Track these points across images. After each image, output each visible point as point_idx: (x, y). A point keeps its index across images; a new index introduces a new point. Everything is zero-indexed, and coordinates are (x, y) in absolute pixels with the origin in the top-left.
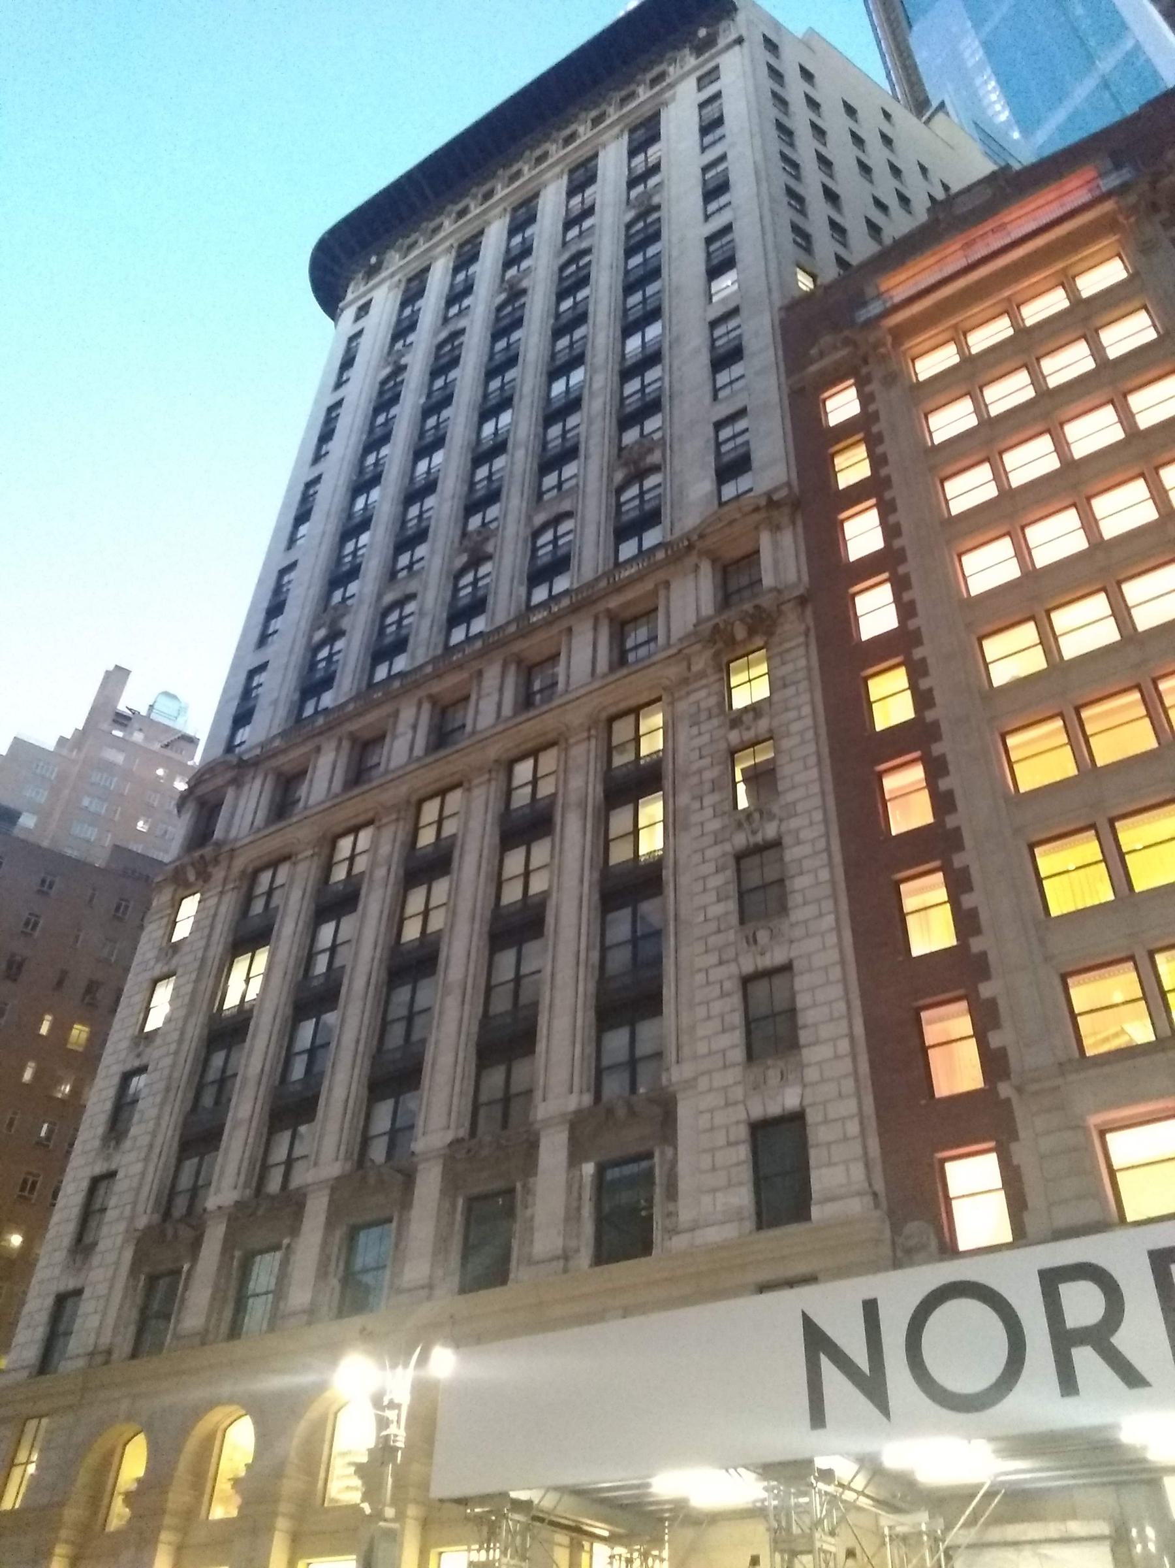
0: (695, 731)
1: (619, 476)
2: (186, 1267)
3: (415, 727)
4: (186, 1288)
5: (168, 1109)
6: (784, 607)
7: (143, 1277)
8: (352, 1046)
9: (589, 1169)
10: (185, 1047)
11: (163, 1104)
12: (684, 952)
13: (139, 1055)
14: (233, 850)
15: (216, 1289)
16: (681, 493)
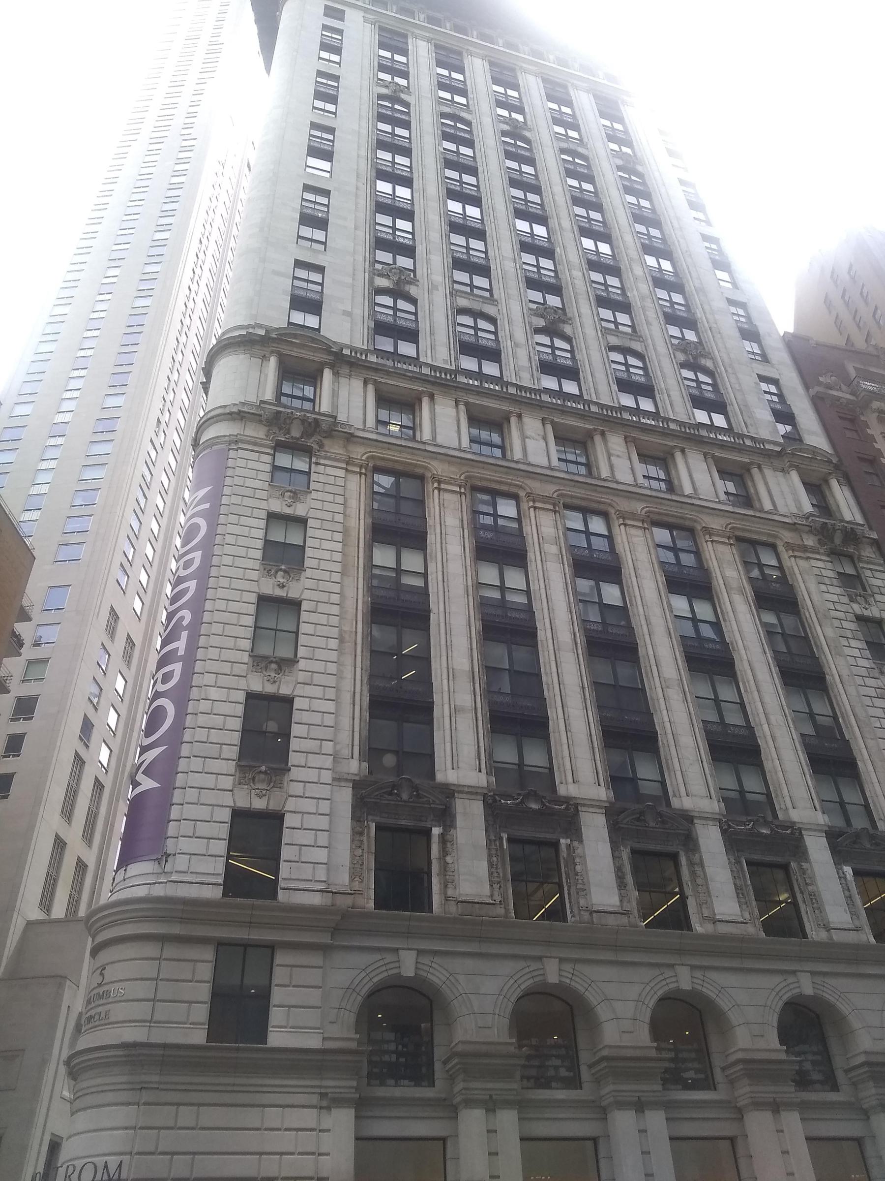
0: (823, 588)
1: (681, 357)
2: (436, 831)
3: (545, 438)
4: (444, 852)
5: (348, 660)
6: (865, 540)
7: (373, 826)
8: (578, 689)
10: (350, 604)
11: (340, 650)
12: (871, 743)
13: (282, 586)
14: (352, 435)
15: (491, 865)
16: (746, 406)
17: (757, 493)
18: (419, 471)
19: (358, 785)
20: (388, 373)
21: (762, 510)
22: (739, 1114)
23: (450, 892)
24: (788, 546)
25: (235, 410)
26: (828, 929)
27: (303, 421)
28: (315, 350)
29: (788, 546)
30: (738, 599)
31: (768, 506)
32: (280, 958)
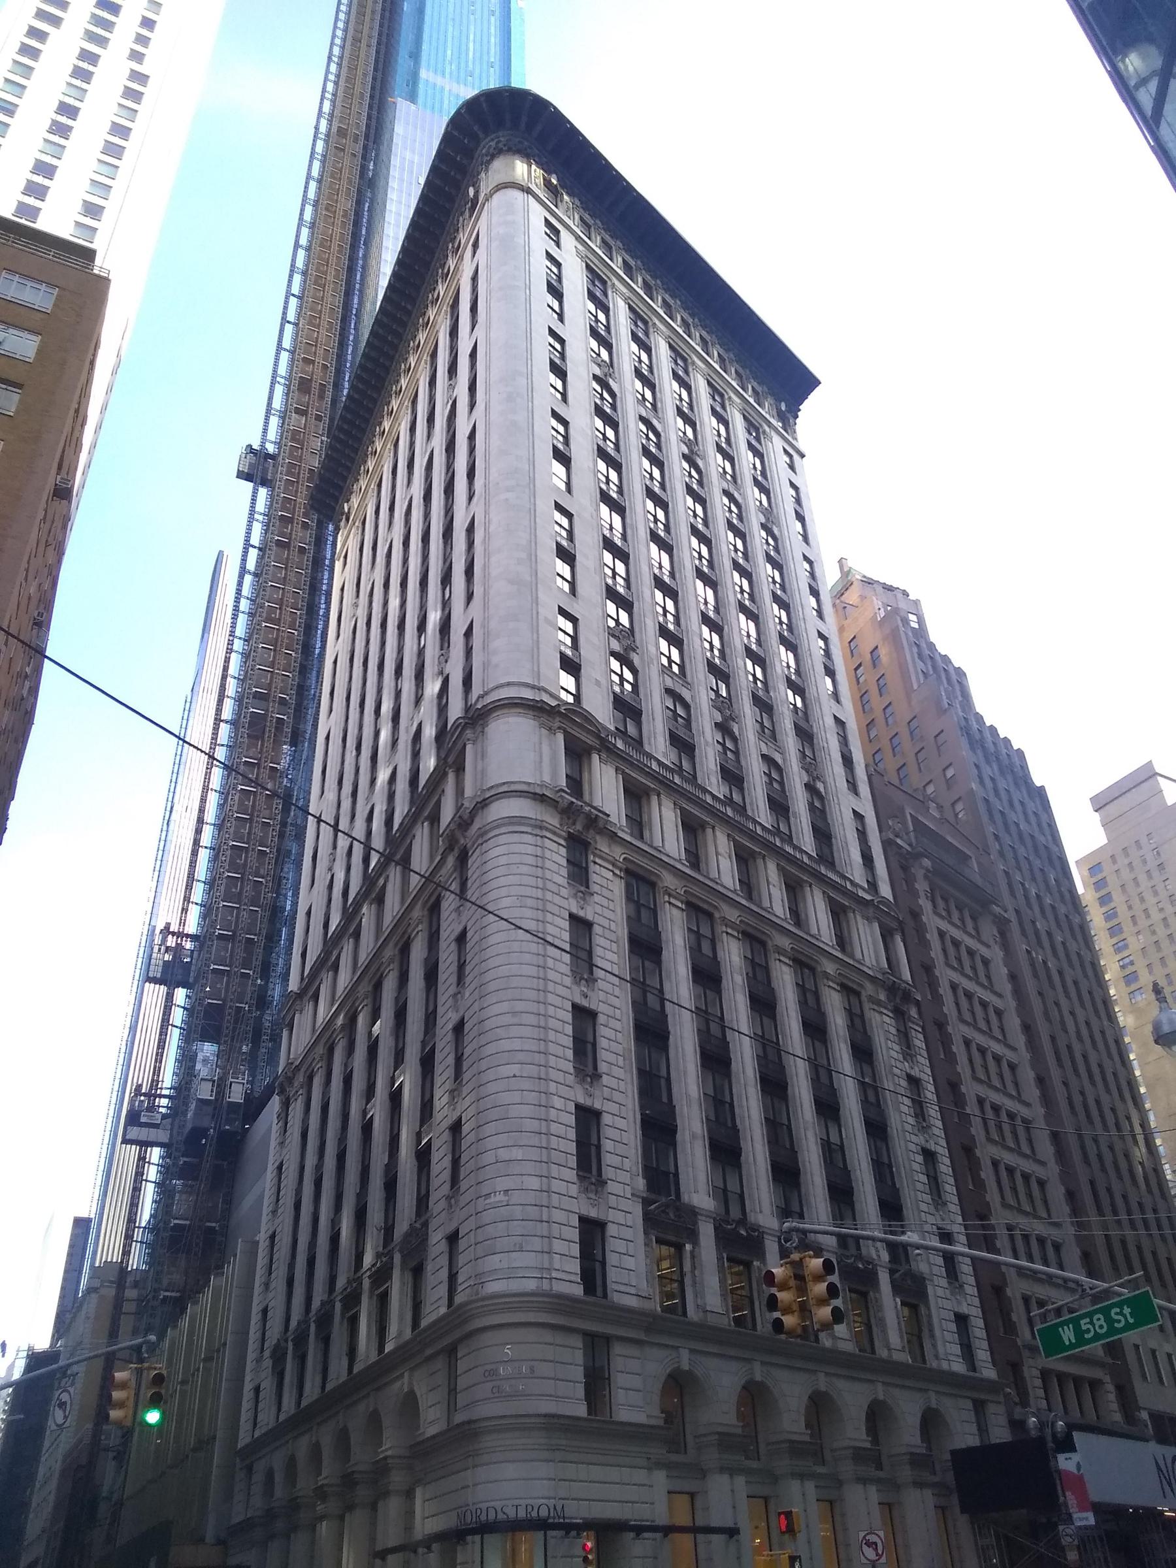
2: (688, 1247)
9: (898, 1300)
17: (850, 937)
18: (653, 878)
19: (646, 1202)
20: (632, 764)
21: (852, 956)
22: (840, 1484)
23: (699, 1302)
24: (871, 999)
25: (538, 791)
26: (889, 1349)
27: (588, 816)
28: (589, 731)
29: (871, 999)
30: (843, 1046)
31: (859, 956)
32: (618, 1349)
